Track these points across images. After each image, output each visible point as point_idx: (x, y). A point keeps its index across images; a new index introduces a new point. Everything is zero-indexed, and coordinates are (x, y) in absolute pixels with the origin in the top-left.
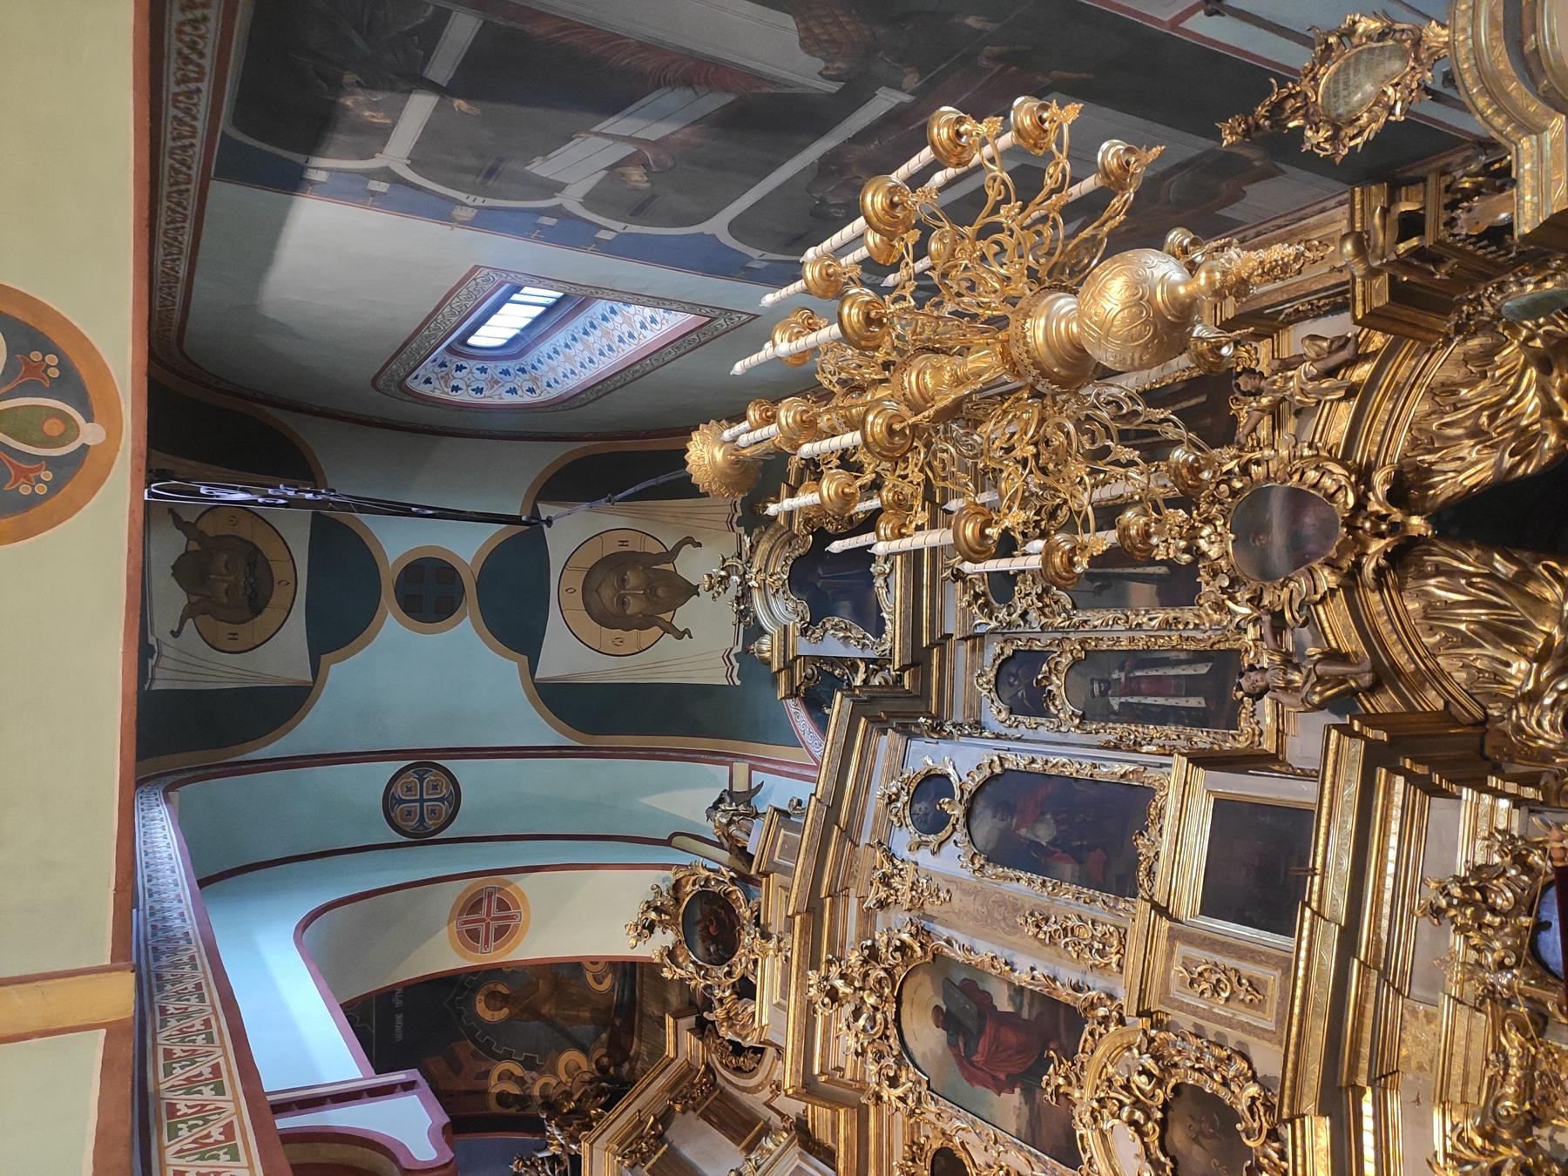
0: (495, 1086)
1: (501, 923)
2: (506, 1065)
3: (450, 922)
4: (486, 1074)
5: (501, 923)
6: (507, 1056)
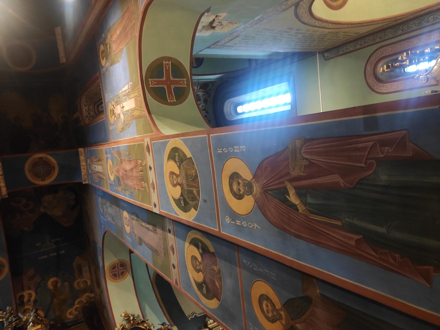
0: (26, 294)
1: (118, 275)
2: (34, 294)
3: (118, 260)
4: (30, 289)
5: (118, 275)
6: (37, 293)
